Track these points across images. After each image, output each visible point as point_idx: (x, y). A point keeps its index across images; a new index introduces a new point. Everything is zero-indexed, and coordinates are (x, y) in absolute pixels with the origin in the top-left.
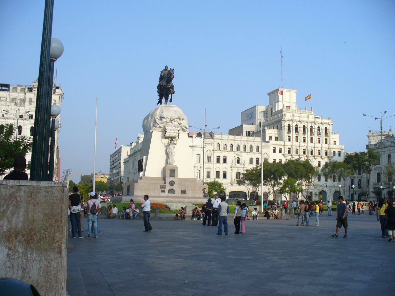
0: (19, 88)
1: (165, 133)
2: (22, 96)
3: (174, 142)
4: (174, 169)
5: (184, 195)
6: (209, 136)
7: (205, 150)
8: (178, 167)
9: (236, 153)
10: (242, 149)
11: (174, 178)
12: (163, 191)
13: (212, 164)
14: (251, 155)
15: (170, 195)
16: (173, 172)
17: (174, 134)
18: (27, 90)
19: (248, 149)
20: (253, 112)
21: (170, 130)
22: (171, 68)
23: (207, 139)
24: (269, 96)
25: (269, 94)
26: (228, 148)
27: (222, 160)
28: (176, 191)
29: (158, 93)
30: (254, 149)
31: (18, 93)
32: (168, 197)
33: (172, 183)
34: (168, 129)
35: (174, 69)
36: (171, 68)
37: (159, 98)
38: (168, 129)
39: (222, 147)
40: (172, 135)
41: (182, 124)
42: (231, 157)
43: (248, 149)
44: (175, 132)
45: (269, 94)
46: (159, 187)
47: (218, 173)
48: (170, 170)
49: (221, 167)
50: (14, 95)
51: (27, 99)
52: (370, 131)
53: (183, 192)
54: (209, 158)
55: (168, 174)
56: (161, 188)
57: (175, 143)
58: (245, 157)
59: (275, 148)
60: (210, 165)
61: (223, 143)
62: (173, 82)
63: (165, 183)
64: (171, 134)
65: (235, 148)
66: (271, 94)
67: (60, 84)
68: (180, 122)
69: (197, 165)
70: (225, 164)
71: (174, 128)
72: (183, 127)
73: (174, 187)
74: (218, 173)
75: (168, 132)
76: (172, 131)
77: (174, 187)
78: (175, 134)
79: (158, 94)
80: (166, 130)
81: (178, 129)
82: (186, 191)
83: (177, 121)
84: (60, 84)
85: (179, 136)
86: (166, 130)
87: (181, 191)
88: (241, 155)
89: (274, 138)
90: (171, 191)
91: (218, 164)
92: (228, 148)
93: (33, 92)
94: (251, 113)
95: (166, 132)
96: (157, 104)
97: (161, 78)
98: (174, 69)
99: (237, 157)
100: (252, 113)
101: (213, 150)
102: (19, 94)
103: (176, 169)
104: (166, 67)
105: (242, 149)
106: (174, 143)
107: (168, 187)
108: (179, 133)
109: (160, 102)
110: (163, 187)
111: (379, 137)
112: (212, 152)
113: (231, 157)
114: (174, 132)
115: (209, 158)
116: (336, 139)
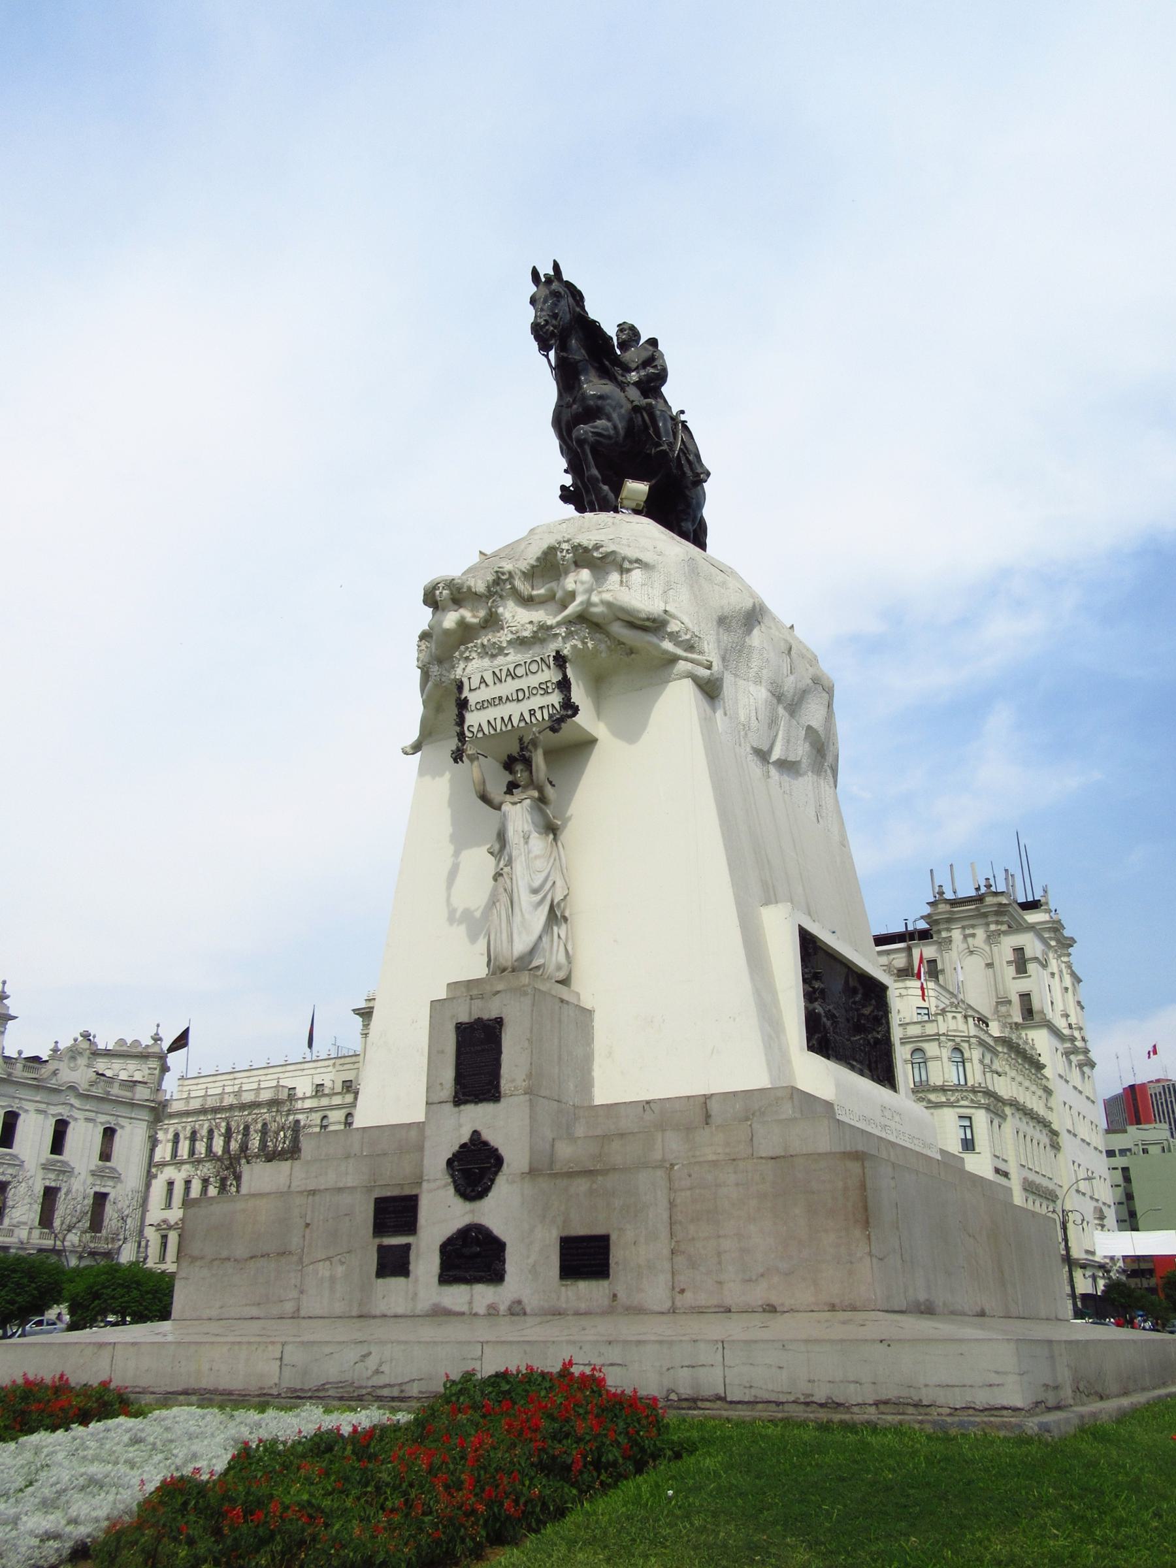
1: (461, 720)
5: (587, 1291)
15: (457, 1296)
17: (525, 707)
21: (489, 678)
22: (535, 274)
32: (440, 1313)
35: (556, 266)
36: (535, 274)
38: (475, 682)
41: (579, 599)
44: (534, 681)
46: (365, 1214)
56: (380, 1228)
64: (504, 710)
67: (1045, 892)
71: (513, 657)
75: (482, 706)
76: (508, 688)
78: (536, 702)
80: (460, 686)
81: (550, 649)
82: (613, 1238)
86: (466, 693)
87: (561, 1238)
98: (556, 266)
108: (564, 685)
114: (522, 683)
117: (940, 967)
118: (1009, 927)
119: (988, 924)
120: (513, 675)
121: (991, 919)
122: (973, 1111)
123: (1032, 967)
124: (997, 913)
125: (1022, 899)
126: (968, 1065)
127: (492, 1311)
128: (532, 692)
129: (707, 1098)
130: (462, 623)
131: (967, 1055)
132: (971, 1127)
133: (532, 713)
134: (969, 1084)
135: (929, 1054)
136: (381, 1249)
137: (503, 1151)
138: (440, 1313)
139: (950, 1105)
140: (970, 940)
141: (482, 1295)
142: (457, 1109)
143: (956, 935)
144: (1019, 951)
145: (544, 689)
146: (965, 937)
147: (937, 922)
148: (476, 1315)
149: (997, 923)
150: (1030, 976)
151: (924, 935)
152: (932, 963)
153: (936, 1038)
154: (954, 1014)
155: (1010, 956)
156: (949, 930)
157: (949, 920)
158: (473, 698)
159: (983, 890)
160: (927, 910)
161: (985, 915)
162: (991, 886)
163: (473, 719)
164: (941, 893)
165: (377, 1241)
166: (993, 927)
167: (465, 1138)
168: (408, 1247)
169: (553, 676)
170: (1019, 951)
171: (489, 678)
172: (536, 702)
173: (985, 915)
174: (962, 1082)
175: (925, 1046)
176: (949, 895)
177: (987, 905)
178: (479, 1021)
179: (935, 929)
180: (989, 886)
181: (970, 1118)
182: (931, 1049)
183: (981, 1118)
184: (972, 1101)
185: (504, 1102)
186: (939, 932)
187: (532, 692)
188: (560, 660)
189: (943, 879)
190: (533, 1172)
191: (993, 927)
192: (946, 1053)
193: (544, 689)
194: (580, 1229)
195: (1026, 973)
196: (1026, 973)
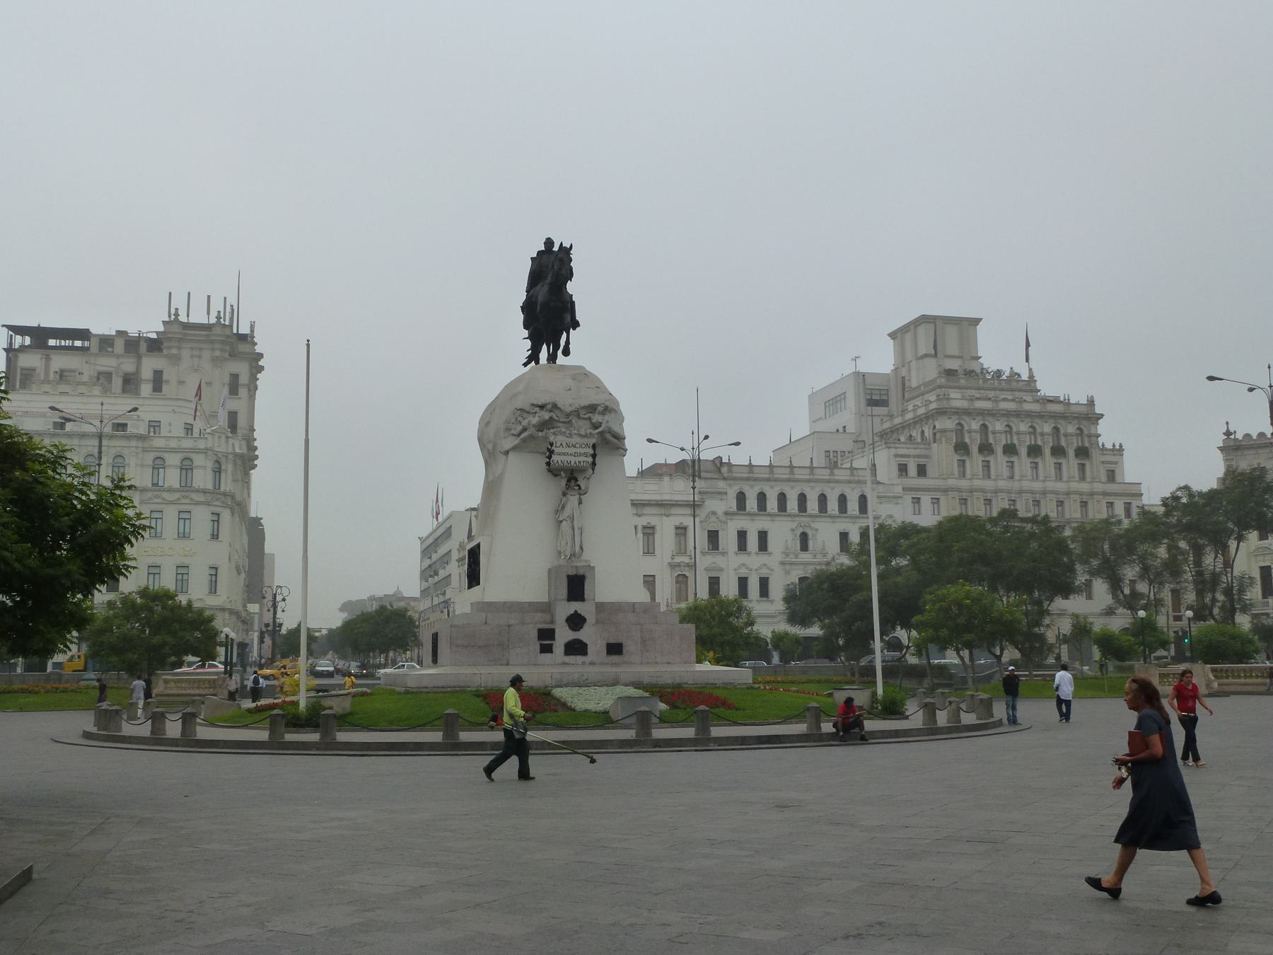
0: (119, 346)
1: (550, 457)
2: (128, 366)
3: (578, 485)
4: (581, 572)
5: (615, 658)
6: (710, 472)
7: (702, 513)
8: (594, 568)
9: (797, 519)
10: (813, 506)
11: (581, 603)
12: (547, 649)
13: (724, 554)
14: (844, 525)
16: (576, 586)
18: (143, 347)
19: (833, 506)
20: (845, 393)
21: (564, 446)
22: (561, 244)
23: (706, 479)
24: (892, 342)
25: (893, 335)
26: (772, 505)
27: (752, 542)
28: (588, 647)
29: (526, 327)
30: (853, 506)
31: (118, 357)
32: (564, 664)
33: (576, 621)
34: (558, 444)
35: (571, 246)
37: (528, 344)
38: (558, 444)
39: (752, 504)
40: (573, 460)
41: (603, 426)
42: (782, 533)
43: (833, 506)
44: (582, 451)
45: (893, 335)
46: (535, 634)
47: (743, 582)
48: (568, 576)
49: (754, 563)
50: (106, 363)
51: (147, 373)
52: (1228, 433)
53: (615, 649)
54: (713, 537)
55: (563, 591)
56: (540, 638)
57: (583, 488)
58: (826, 536)
59: (919, 499)
60: (718, 559)
61: (757, 489)
62: (571, 287)
63: (552, 622)
65: (792, 505)
66: (899, 334)
67: (252, 327)
68: (597, 418)
69: (678, 559)
70: (764, 558)
71: (576, 440)
72: (608, 436)
73: (584, 634)
74: (743, 582)
76: (572, 450)
77: (584, 634)
78: (582, 459)
79: (526, 334)
80: (552, 444)
81: (593, 441)
82: (624, 643)
83: (586, 416)
84: (252, 327)
85: (594, 464)
88: (813, 525)
89: (912, 470)
90: (575, 648)
91: (743, 558)
92: (772, 505)
93: (165, 352)
94: (840, 395)
95: (551, 452)
96: (525, 365)
97: (535, 277)
98: (571, 246)
99: (801, 530)
100: (842, 397)
101: (726, 513)
102: (122, 360)
103: (587, 575)
104: (549, 243)
105: (813, 506)
106: (580, 488)
107: (564, 635)
108: (594, 456)
109: (534, 357)
110: (546, 635)
111: (1260, 451)
112: (723, 518)
113: (782, 533)
114: (579, 450)
115: (713, 537)
116: (1116, 463)
117: (165, 377)
118: (230, 355)
119: (213, 350)
120: (575, 447)
121: (217, 346)
122: (192, 507)
123: (243, 392)
124: (223, 342)
125: (235, 331)
126: (223, 475)
127: (584, 663)
128: (580, 455)
129: (634, 603)
130: (551, 418)
131: (223, 467)
132: (218, 521)
133: (580, 462)
134: (223, 488)
135: (196, 464)
136: (541, 645)
137: (586, 617)
138: (564, 664)
139: (207, 504)
140: (196, 360)
141: (580, 659)
142: (567, 603)
143: (186, 354)
144: (235, 377)
145: (586, 455)
146: (192, 356)
147: (170, 339)
148: (578, 664)
149: (222, 350)
150: (240, 398)
151: (155, 345)
152: (158, 375)
153: (205, 451)
154: (220, 434)
155: (227, 380)
156: (179, 348)
157: (180, 340)
158: (556, 450)
159: (213, 320)
160: (161, 329)
161: (212, 342)
162: (221, 318)
163: (554, 458)
164: (177, 315)
165: (539, 642)
166: (217, 353)
167: (572, 612)
168: (551, 645)
169: (591, 452)
170: (235, 377)
171: (564, 445)
172: (582, 459)
173: (212, 342)
174: (217, 487)
175: (193, 456)
176: (183, 318)
177: (216, 335)
178: (576, 576)
179: (165, 344)
180: (218, 318)
181: (218, 515)
182: (199, 460)
183: (226, 516)
184: (223, 502)
185: (585, 602)
186: (170, 348)
187: (580, 455)
188: (594, 447)
189: (179, 302)
190: (597, 622)
191: (217, 353)
192: (210, 465)
193: (586, 455)
194: (612, 641)
195: (237, 395)
196: (237, 395)
